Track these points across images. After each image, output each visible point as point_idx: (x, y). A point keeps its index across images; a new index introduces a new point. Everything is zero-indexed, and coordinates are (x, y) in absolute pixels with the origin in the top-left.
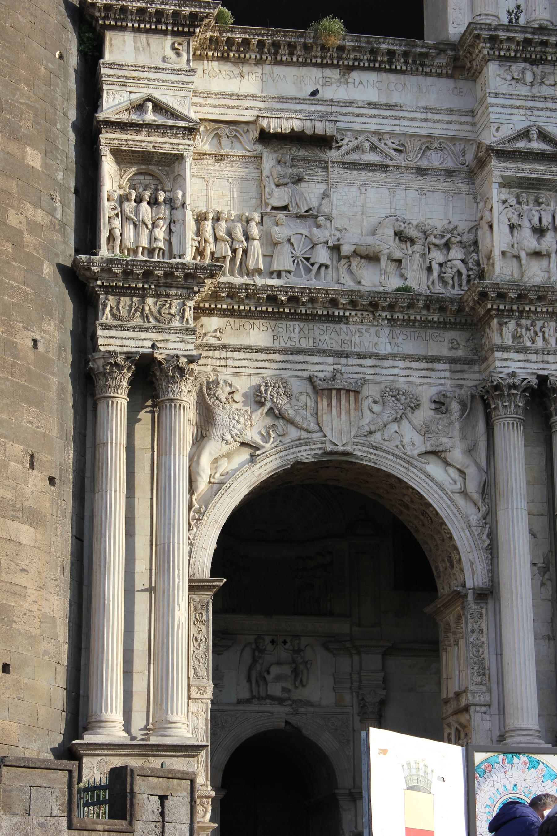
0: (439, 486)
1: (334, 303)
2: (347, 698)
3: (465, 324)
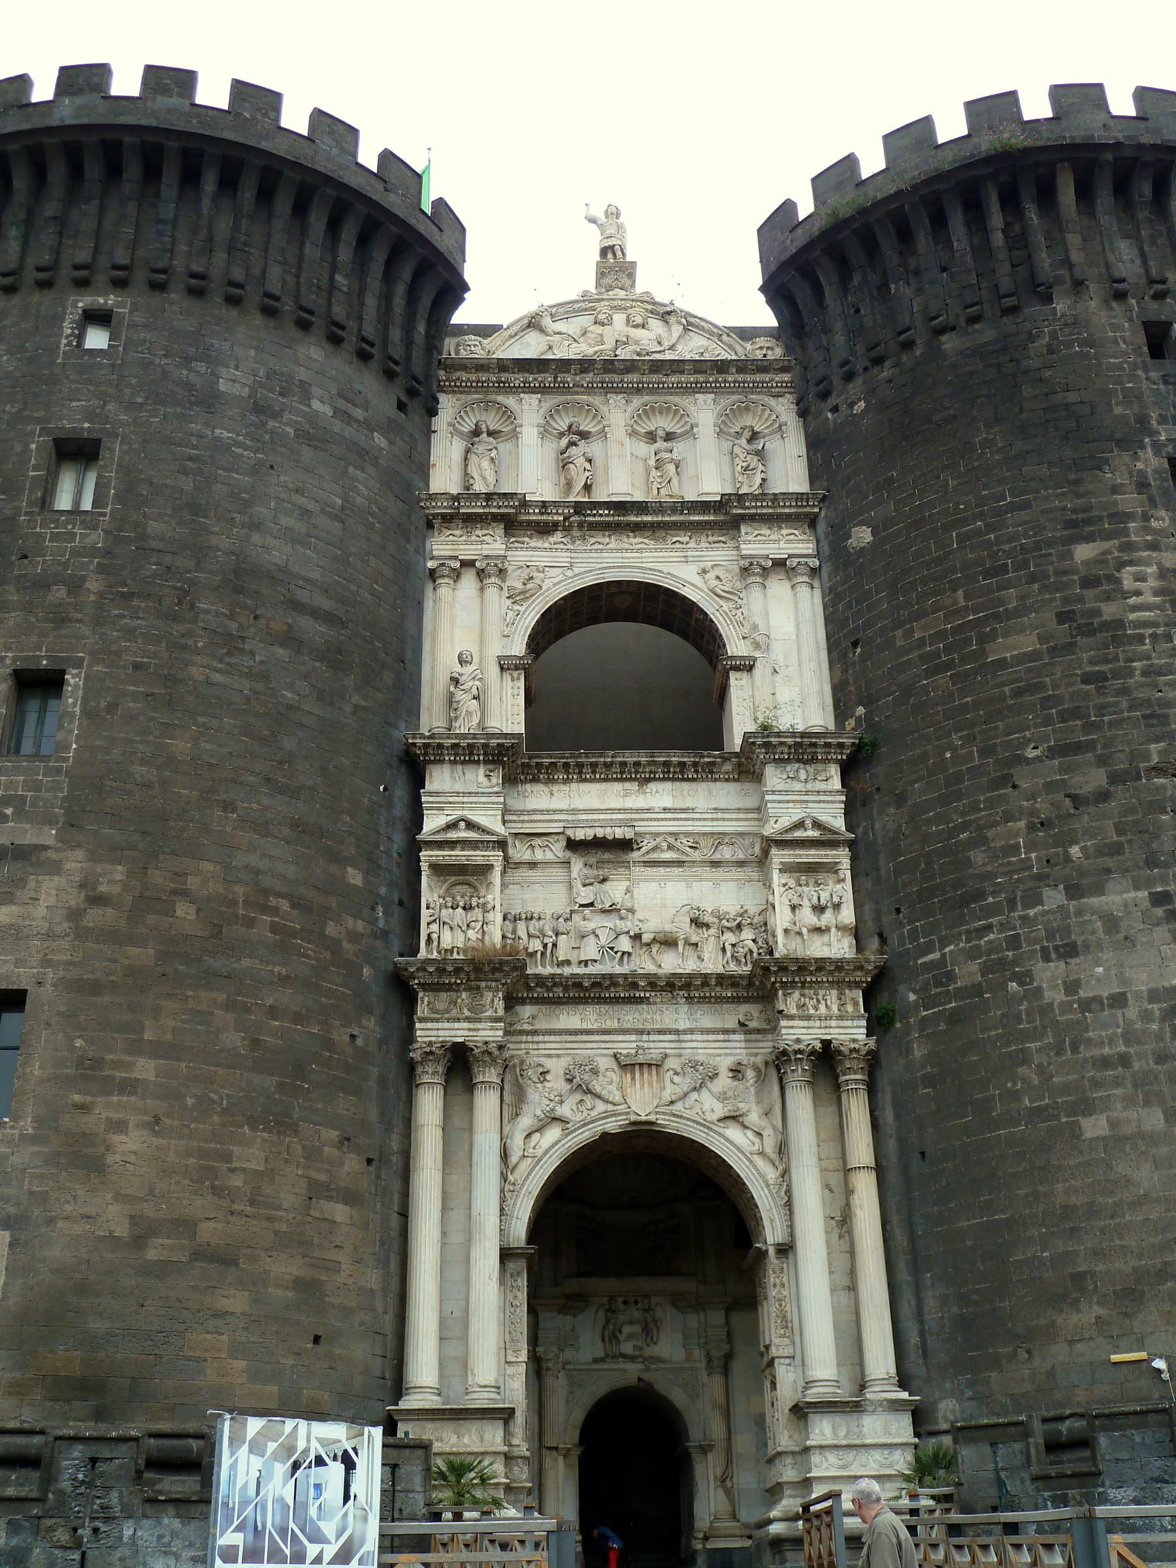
0: (738, 1149)
1: (634, 986)
3: (758, 996)
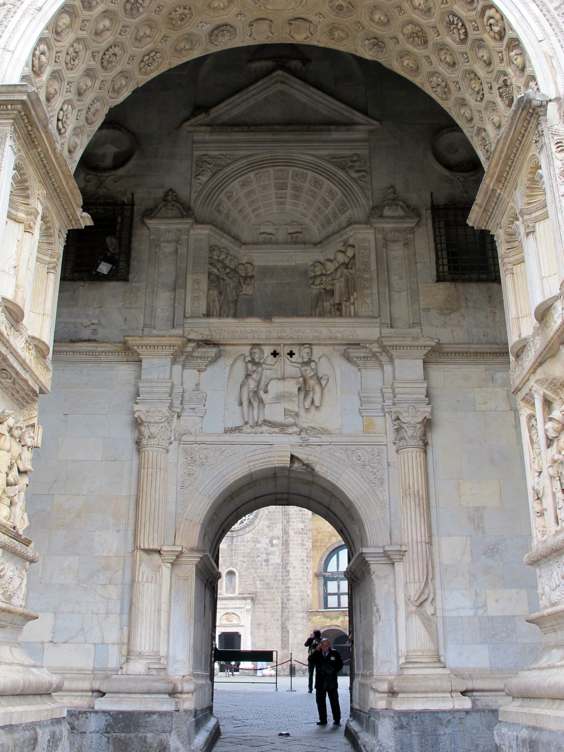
2: (379, 422)
